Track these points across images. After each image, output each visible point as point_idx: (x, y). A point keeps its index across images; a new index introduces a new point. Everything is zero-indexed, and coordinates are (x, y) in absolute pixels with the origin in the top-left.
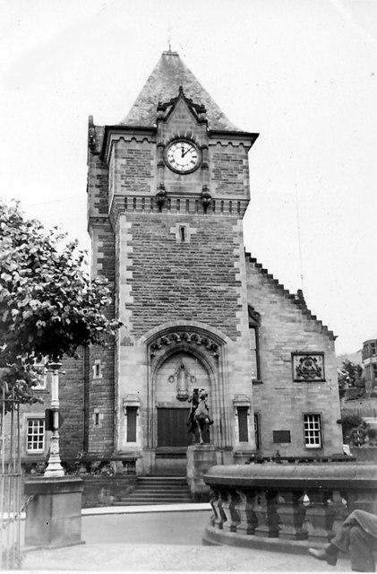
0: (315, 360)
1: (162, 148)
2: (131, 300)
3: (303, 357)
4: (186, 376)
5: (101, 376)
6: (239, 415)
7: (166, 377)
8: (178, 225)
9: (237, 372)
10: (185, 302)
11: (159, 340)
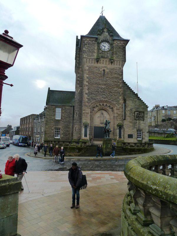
1: (99, 44)
2: (87, 92)
3: (138, 113)
4: (103, 117)
5: (77, 116)
7: (97, 117)
8: (103, 68)
10: (104, 93)
11: (95, 105)
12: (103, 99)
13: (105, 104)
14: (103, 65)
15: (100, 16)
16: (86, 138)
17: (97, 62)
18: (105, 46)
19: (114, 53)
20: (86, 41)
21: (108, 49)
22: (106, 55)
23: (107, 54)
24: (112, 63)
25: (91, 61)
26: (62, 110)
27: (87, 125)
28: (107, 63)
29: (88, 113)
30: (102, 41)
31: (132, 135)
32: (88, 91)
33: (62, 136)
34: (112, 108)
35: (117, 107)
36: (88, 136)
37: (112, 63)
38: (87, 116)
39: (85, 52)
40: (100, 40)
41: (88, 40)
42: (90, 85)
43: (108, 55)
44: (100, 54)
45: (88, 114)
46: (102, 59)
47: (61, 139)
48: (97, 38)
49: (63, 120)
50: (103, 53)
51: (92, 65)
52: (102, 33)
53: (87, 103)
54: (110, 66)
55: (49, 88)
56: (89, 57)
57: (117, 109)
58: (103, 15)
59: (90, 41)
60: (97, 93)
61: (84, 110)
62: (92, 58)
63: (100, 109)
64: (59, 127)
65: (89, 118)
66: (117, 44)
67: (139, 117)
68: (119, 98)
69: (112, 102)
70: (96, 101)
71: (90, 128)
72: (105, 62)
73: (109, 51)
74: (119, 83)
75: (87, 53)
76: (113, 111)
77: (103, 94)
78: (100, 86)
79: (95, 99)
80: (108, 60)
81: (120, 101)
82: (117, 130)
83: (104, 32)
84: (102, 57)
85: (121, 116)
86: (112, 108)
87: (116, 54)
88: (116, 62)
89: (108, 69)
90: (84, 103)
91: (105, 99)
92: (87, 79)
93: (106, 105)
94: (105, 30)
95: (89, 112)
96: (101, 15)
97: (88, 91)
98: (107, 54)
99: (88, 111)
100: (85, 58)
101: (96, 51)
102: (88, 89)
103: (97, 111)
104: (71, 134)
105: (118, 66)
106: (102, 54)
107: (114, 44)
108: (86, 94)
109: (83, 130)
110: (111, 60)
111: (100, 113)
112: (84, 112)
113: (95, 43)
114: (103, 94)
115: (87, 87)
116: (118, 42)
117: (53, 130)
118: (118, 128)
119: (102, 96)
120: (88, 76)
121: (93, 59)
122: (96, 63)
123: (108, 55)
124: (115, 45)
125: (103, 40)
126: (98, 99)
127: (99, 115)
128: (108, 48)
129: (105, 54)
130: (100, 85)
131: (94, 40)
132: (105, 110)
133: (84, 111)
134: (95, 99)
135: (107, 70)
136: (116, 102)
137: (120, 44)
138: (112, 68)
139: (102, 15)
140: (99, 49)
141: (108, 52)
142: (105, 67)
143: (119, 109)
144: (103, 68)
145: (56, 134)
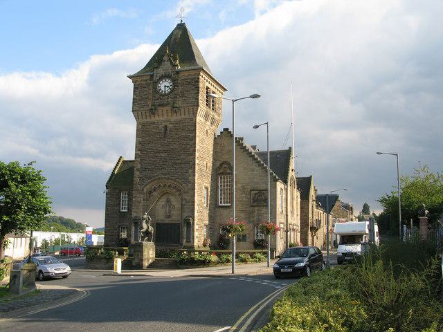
0: (264, 194)
7: (161, 206)
10: (164, 166)
18: (165, 86)
28: (170, 114)
29: (139, 202)
43: (169, 99)
48: (152, 76)
54: (174, 118)
56: (141, 109)
61: (135, 197)
66: (184, 78)
67: (257, 200)
74: (188, 146)
84: (160, 105)
88: (182, 110)
101: (151, 97)
103: (159, 196)
106: (159, 101)
108: (138, 170)
111: (164, 200)
119: (161, 172)
123: (169, 99)
125: (162, 75)
127: (163, 203)
135: (170, 126)
140: (156, 91)
142: (168, 121)
143: (187, 192)
144: (163, 124)
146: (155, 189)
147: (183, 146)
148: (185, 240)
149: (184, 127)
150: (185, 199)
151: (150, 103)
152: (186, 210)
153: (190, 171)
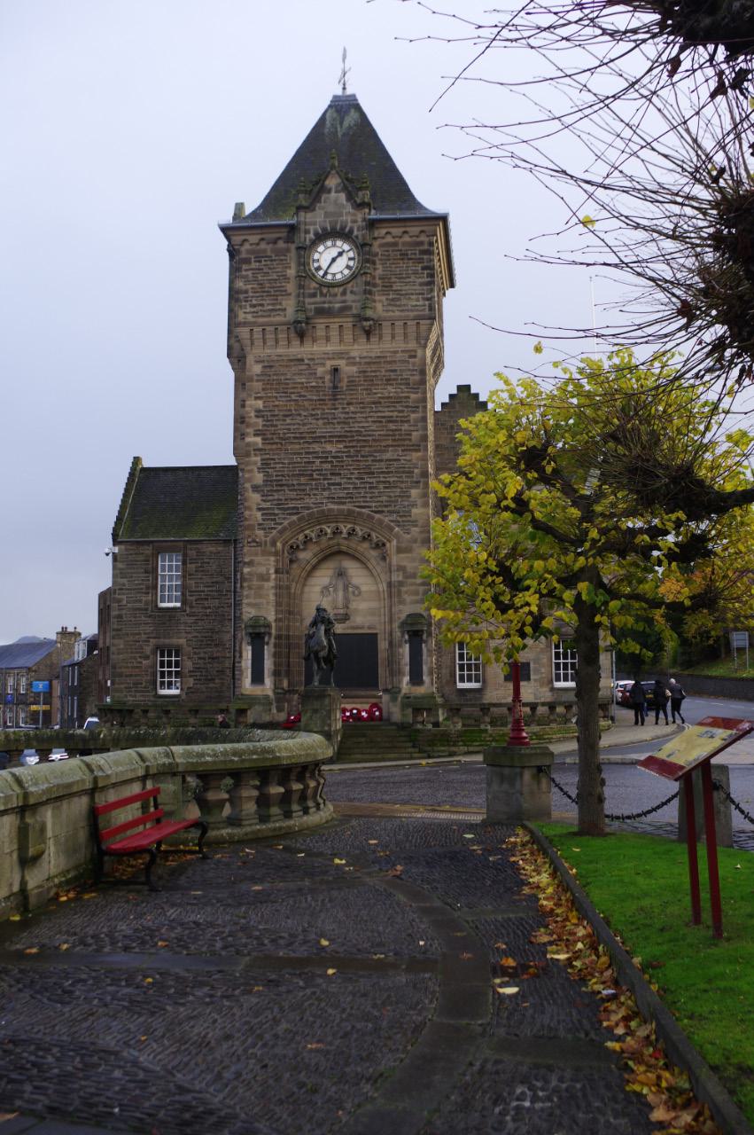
1: (305, 250)
6: (410, 642)
7: (318, 589)
9: (410, 581)
10: (337, 479)
11: (301, 537)
12: (336, 507)
13: (345, 529)
14: (329, 348)
15: (336, 99)
16: (257, 691)
17: (301, 335)
19: (375, 285)
20: (247, 246)
21: (346, 272)
22: (339, 298)
23: (344, 293)
24: (368, 333)
25: (270, 336)
26: (184, 563)
27: (262, 630)
28: (348, 337)
29: (264, 578)
30: (316, 234)
31: (528, 664)
32: (262, 475)
33: (191, 682)
34: (379, 546)
35: (397, 536)
36: (268, 681)
37: (368, 333)
38: (261, 588)
39: (241, 296)
40: (307, 232)
41: (254, 239)
42: (274, 447)
43: (349, 297)
44: (313, 300)
45: (268, 580)
46: (320, 323)
47: (184, 697)
48: (292, 229)
49: (191, 607)
50: (325, 290)
51: (280, 351)
52: (317, 199)
53: (262, 532)
54: (360, 349)
55: (137, 460)
57: (399, 550)
58: (349, 92)
59: (263, 246)
60: (303, 480)
61: (250, 564)
62: (278, 319)
63: (328, 552)
64: (175, 641)
65: (272, 598)
66: (389, 239)
68: (409, 496)
69: (377, 516)
70: (299, 519)
71: (275, 646)
72: (334, 333)
73: (353, 277)
74: (405, 427)
75: (254, 302)
76: (384, 559)
77: (333, 484)
78: (317, 447)
79: (295, 511)
80: (348, 322)
81: (414, 511)
82: (400, 646)
83: (329, 191)
84: (321, 312)
85: (419, 581)
86: (379, 546)
87: (388, 287)
88: (386, 326)
89: (354, 364)
90: (247, 533)
91: (342, 507)
92: (260, 421)
93: (352, 533)
94: (332, 182)
95: (272, 571)
96: (339, 92)
97: (262, 475)
98: (344, 293)
99: (267, 565)
100: (245, 324)
101: (291, 287)
102: (265, 464)
103: (314, 561)
104: (228, 672)
105: (399, 345)
106: (318, 299)
107: (376, 243)
108: (256, 488)
109: (248, 653)
110: (361, 318)
111: (330, 572)
112: (249, 573)
113: (288, 250)
114: (333, 484)
115: (259, 458)
116: (396, 231)
117: (147, 658)
118: (407, 637)
119: (326, 494)
120: (260, 404)
121: (280, 328)
122: (296, 342)
123: (349, 297)
124: (382, 245)
125: (324, 229)
126: (308, 508)
127: (326, 581)
128: (348, 267)
129: (336, 295)
130: (317, 440)
131: (280, 238)
132: (354, 558)
133: (246, 570)
134: (295, 511)
135: (348, 370)
136: (394, 517)
137: (407, 239)
138: (373, 355)
139: (344, 88)
140: (306, 273)
141: (350, 285)
142: (340, 355)
144: (329, 364)
145: (162, 673)
146: (307, 541)
147: (392, 426)
148: (406, 679)
149: (393, 375)
150: (401, 568)
151: (290, 305)
152: (408, 598)
153: (414, 492)
